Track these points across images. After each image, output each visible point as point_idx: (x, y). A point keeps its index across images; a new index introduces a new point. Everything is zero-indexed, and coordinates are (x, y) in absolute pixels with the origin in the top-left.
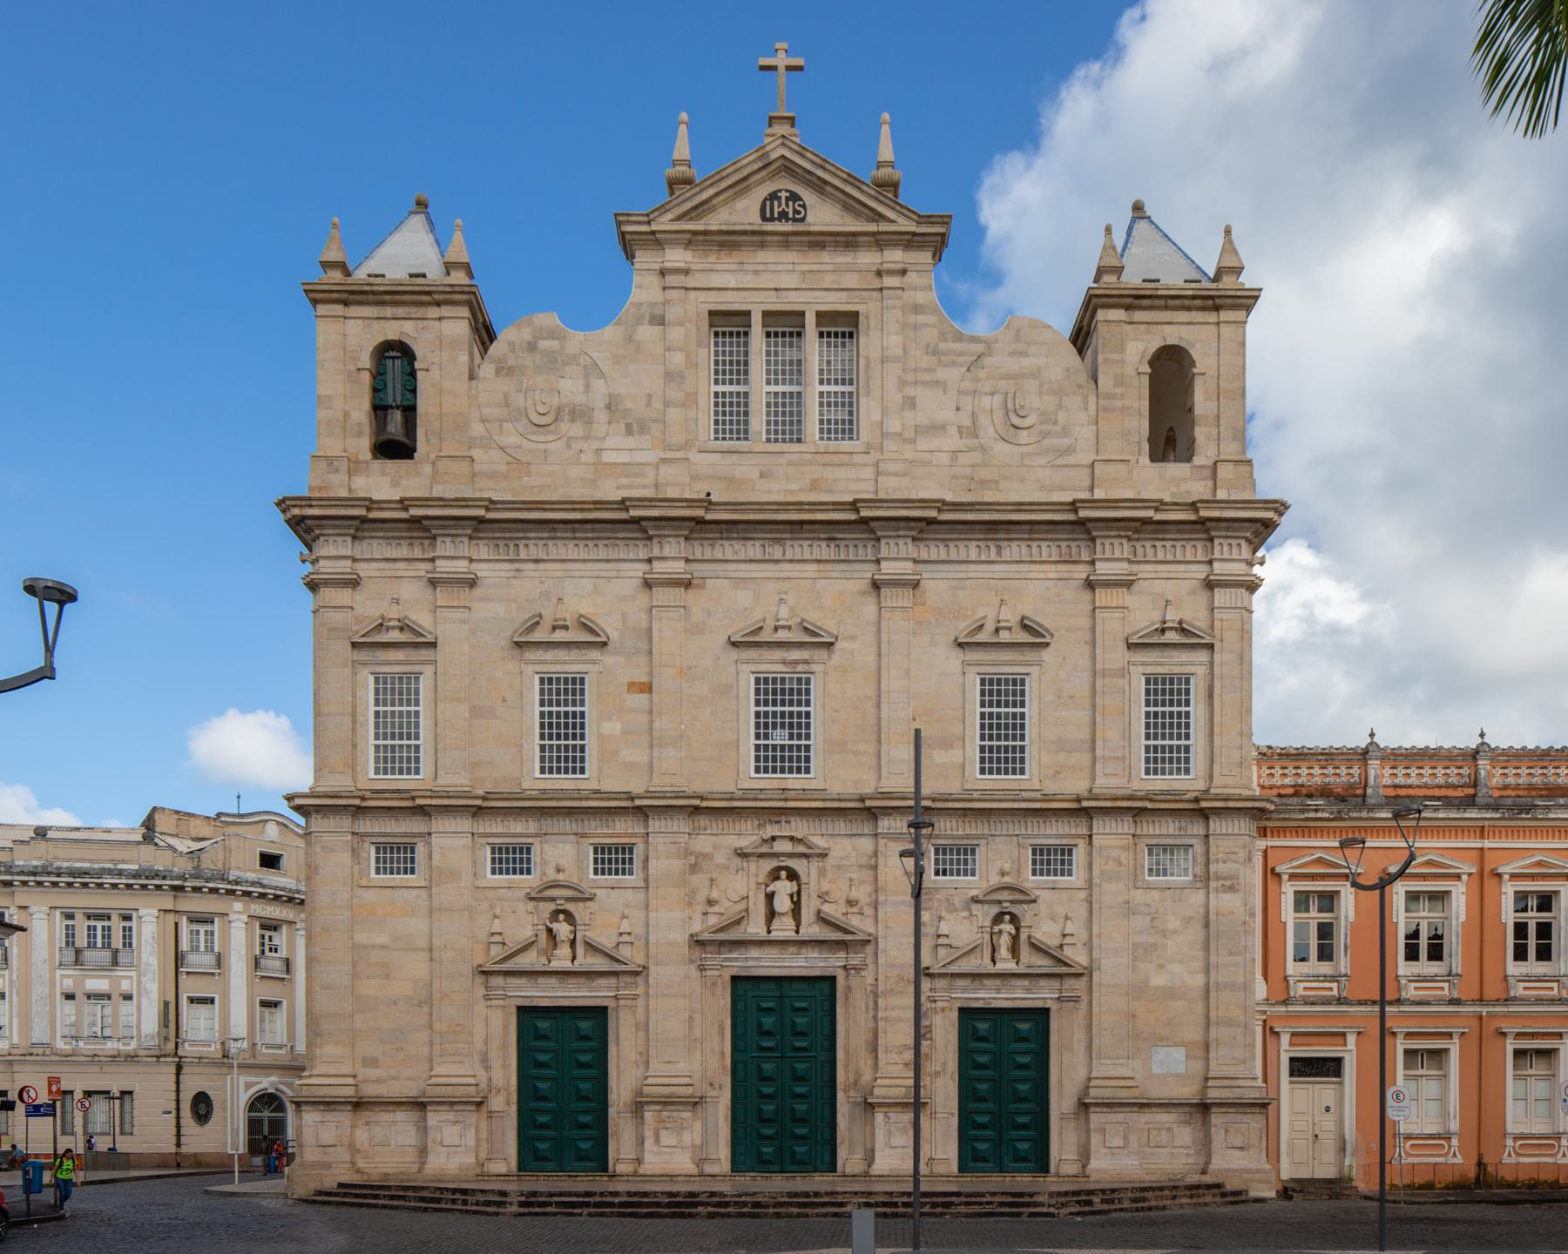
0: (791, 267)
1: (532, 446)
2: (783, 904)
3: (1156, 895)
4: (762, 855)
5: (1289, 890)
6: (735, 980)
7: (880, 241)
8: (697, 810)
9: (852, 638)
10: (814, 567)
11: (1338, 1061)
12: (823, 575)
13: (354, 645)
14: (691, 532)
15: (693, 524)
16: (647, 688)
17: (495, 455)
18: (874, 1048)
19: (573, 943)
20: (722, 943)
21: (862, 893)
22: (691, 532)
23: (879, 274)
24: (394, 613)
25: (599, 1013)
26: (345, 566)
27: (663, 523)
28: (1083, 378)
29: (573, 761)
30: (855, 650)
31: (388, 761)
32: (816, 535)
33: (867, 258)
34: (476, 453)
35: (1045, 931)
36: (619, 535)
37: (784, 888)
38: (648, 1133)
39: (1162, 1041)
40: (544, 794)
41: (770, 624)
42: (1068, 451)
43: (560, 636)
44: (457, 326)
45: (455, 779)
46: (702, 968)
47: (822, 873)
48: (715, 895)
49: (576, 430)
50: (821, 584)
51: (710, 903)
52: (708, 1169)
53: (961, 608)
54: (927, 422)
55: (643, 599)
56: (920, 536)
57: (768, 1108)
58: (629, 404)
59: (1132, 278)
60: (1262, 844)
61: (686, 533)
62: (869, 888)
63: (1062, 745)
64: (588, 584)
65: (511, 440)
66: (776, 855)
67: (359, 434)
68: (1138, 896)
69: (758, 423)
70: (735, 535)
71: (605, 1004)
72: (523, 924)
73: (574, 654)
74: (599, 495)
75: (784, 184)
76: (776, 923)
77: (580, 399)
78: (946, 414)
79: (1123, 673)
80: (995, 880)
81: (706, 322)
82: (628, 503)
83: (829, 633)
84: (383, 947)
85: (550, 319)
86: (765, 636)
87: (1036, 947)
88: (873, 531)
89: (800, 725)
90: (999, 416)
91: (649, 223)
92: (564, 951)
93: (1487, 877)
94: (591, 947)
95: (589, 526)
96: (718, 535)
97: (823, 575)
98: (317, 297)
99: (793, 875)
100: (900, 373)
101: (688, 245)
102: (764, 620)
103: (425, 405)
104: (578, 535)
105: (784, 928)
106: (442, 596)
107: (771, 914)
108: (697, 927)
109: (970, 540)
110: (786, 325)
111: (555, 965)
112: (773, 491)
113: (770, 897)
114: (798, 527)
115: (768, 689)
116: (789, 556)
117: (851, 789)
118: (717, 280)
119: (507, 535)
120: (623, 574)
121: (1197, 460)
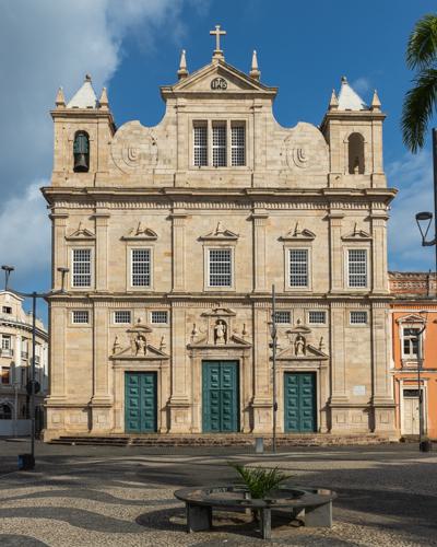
2: (220, 333)
3: (353, 330)
4: (213, 316)
5: (402, 327)
6: (203, 361)
7: (253, 96)
8: (189, 299)
17: (118, 171)
20: (199, 348)
21: (248, 330)
23: (252, 108)
25: (155, 374)
28: (325, 143)
29: (146, 281)
30: (245, 240)
33: (249, 102)
34: (110, 171)
35: (314, 344)
37: (221, 326)
38: (172, 417)
39: (356, 383)
40: (135, 293)
42: (320, 170)
44: (104, 125)
46: (191, 357)
47: (234, 322)
49: (146, 162)
50: (233, 217)
52: (194, 431)
57: (216, 408)
59: (341, 109)
60: (391, 311)
62: (251, 327)
63: (319, 275)
65: (122, 166)
66: (218, 316)
67: (69, 163)
68: (347, 330)
69: (211, 160)
72: (125, 342)
73: (145, 243)
74: (155, 186)
76: (218, 341)
77: (146, 152)
78: (277, 157)
79: (341, 249)
80: (296, 325)
81: (191, 125)
85: (137, 123)
86: (213, 236)
87: (312, 350)
89: (227, 268)
90: (296, 157)
92: (142, 350)
94: (152, 350)
98: (54, 116)
99: (224, 323)
101: (186, 98)
103: (92, 153)
105: (221, 343)
107: (216, 337)
108: (188, 342)
110: (220, 127)
111: (139, 356)
112: (216, 184)
113: (216, 331)
115: (214, 255)
117: (244, 291)
118: (196, 109)
121: (366, 173)
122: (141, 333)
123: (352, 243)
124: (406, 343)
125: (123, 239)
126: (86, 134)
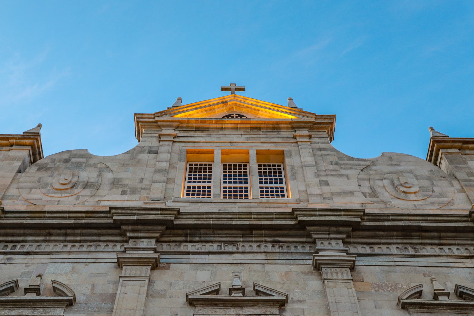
0: (240, 136)
1: (49, 199)
9: (300, 301)
10: (263, 257)
12: (270, 262)
14: (162, 235)
15: (164, 228)
22: (162, 235)
27: (140, 227)
32: (263, 239)
36: (102, 238)
41: (225, 288)
53: (397, 284)
54: (340, 191)
55: (114, 275)
56: (348, 240)
58: (127, 182)
61: (157, 235)
64: (68, 267)
70: (197, 239)
82: (113, 211)
83: (279, 293)
88: (309, 236)
91: (154, 118)
95: (79, 231)
96: (183, 239)
97: (270, 262)
100: (316, 171)
102: (220, 285)
104: (69, 238)
109: (390, 244)
114: (248, 232)
116: (240, 250)
119: (10, 239)
120: (99, 260)
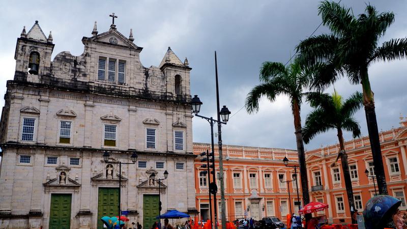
2: (110, 172)
11: (208, 205)
13: (21, 112)
16: (83, 126)
18: (127, 203)
19: (65, 180)
23: (130, 54)
24: (31, 106)
26: (21, 95)
31: (25, 137)
37: (110, 169)
43: (67, 114)
45: (41, 141)
48: (96, 170)
51: (95, 171)
58: (83, 71)
71: (71, 193)
72: (55, 175)
75: (114, 37)
84: (21, 180)
86: (108, 118)
93: (229, 171)
94: (70, 180)
99: (112, 166)
105: (110, 177)
106: (42, 103)
107: (107, 174)
110: (113, 61)
113: (107, 171)
118: (102, 51)
122: (63, 171)
123: (176, 128)
124: (201, 179)
125: (57, 115)
126: (38, 54)
